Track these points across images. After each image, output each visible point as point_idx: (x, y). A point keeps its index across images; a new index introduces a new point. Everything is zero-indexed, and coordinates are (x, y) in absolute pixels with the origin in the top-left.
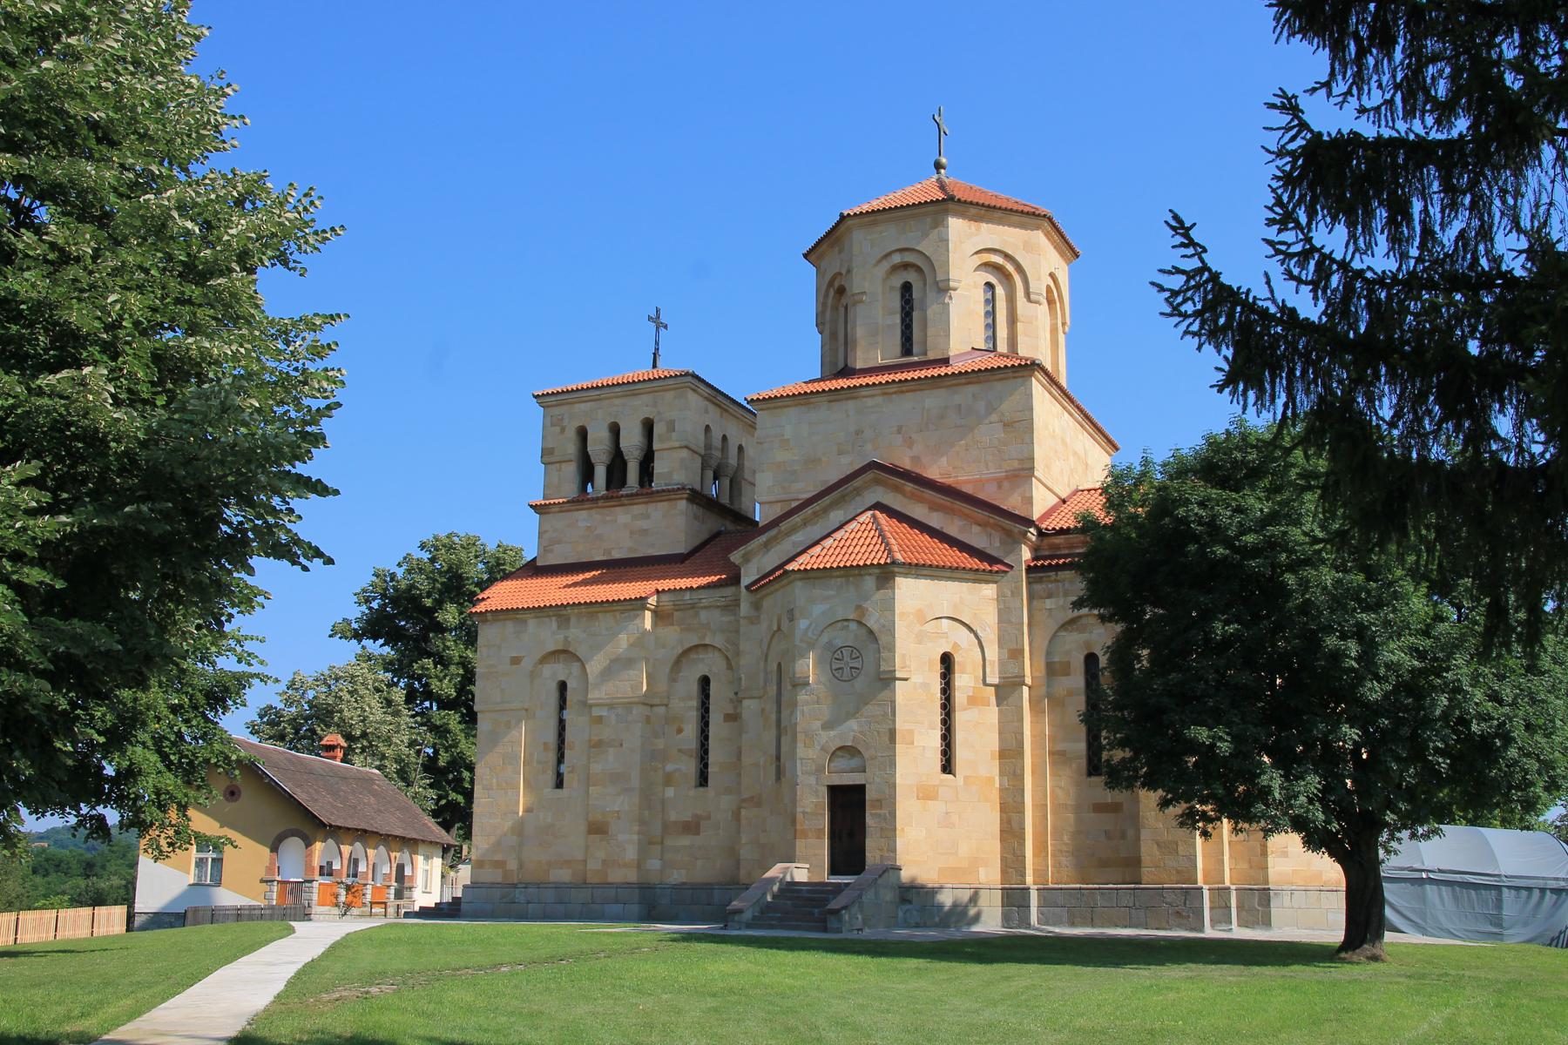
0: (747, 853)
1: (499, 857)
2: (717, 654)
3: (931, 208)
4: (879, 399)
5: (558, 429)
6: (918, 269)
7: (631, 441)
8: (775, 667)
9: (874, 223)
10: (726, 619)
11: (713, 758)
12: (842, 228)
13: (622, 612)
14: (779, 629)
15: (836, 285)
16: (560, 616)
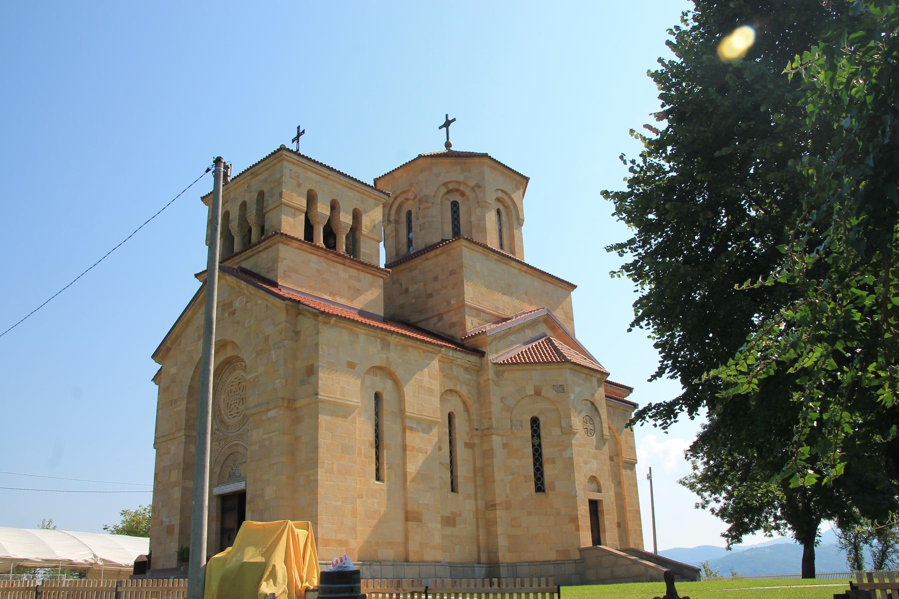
0: (502, 542)
1: (341, 536)
2: (458, 399)
3: (519, 178)
4: (516, 271)
5: (295, 183)
6: (506, 207)
7: (346, 219)
8: (528, 418)
9: (494, 168)
10: (468, 376)
11: (463, 471)
13: (424, 351)
14: (538, 393)
15: (451, 186)
16: (383, 340)
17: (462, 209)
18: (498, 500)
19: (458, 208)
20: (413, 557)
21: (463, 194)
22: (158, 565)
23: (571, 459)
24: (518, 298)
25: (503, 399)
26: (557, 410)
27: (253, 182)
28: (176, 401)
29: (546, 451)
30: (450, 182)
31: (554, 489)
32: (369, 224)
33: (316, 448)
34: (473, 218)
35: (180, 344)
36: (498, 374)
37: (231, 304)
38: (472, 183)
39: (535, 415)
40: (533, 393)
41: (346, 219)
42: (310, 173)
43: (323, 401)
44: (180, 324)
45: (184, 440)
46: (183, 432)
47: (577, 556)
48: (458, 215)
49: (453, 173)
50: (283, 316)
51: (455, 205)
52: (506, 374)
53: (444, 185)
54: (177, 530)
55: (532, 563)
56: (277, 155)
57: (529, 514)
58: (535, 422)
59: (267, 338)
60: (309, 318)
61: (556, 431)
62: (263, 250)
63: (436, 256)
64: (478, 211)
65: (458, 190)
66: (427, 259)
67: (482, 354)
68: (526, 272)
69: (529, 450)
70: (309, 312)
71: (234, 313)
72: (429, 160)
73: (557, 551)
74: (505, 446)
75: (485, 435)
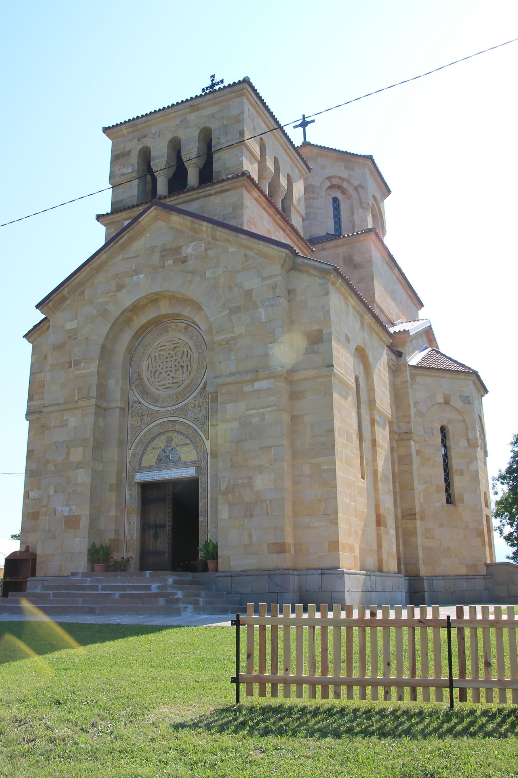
12: (361, 160)
14: (447, 402)
15: (335, 181)
17: (344, 207)
18: (418, 509)
19: (338, 205)
20: (385, 569)
21: (344, 192)
22: (50, 566)
23: (477, 472)
24: (398, 306)
25: (416, 403)
26: (464, 421)
27: (192, 117)
28: (77, 363)
29: (456, 463)
30: (334, 177)
31: (462, 501)
32: (297, 195)
33: (331, 431)
34: (356, 218)
35: (82, 293)
36: (413, 376)
37: (178, 250)
38: (356, 183)
39: (444, 423)
40: (442, 401)
41: (284, 182)
42: (260, 119)
43: (335, 375)
44: (87, 268)
45: (93, 411)
46: (93, 401)
47: (484, 572)
48: (339, 212)
49: (339, 170)
50: (276, 269)
51: (335, 200)
52: (417, 378)
53: (328, 178)
54: (84, 523)
55: (446, 577)
56: (236, 88)
57: (441, 526)
58: (443, 430)
59: (248, 294)
60: (310, 274)
61: (463, 443)
62: (215, 194)
63: (336, 246)
64: (361, 211)
65: (339, 187)
66: (323, 249)
67: (399, 354)
68: (400, 282)
69: (440, 459)
70: (315, 268)
71: (184, 261)
72: (316, 150)
73: (467, 566)
74: (418, 452)
75: (402, 440)
